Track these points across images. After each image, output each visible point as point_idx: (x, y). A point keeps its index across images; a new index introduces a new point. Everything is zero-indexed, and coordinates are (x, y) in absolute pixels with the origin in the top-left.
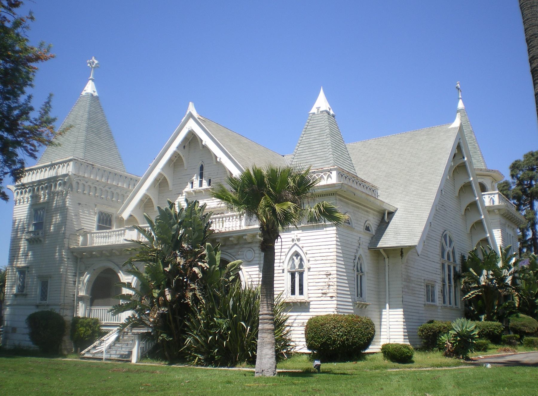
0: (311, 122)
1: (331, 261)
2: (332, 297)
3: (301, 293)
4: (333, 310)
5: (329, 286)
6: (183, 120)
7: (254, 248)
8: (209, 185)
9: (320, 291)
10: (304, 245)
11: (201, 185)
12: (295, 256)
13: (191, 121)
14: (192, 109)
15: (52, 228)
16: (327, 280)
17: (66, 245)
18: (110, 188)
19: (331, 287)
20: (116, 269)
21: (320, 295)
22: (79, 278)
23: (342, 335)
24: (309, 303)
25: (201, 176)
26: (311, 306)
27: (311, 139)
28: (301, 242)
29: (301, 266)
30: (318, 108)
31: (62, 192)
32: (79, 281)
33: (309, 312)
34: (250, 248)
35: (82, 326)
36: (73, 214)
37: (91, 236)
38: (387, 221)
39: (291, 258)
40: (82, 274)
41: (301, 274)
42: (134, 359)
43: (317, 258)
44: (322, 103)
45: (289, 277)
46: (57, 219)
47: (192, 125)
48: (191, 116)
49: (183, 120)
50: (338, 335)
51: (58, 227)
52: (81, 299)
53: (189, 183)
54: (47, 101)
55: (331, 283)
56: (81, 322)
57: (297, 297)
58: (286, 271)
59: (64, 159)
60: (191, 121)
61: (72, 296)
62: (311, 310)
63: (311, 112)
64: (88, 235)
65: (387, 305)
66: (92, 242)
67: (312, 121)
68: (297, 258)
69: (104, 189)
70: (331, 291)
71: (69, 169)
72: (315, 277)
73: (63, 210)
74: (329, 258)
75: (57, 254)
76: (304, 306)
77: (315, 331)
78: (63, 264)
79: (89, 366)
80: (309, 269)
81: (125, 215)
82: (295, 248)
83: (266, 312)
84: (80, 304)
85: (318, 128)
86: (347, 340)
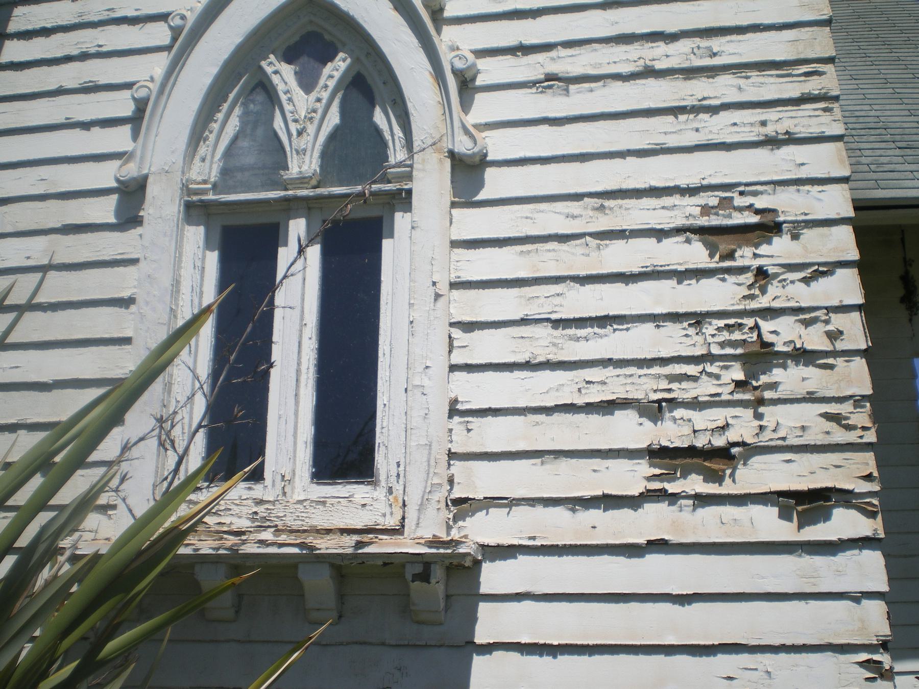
2: (810, 503)
3: (346, 449)
5: (761, 357)
9: (630, 430)
12: (289, 57)
19: (789, 378)
21: (633, 477)
24: (455, 573)
26: (491, 623)
29: (355, 146)
39: (243, 79)
55: (783, 332)
58: (162, 204)
68: (308, 83)
70: (785, 420)
72: (549, 259)
80: (468, 171)
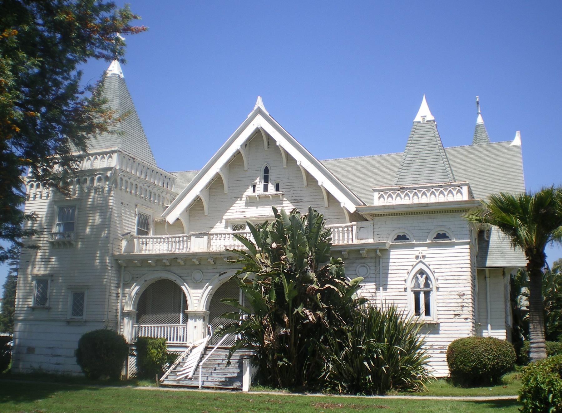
0: (416, 131)
1: (465, 281)
2: (466, 319)
3: (428, 313)
4: (469, 332)
5: (463, 307)
6: (249, 116)
7: (368, 264)
8: (277, 190)
9: (452, 312)
10: (431, 263)
11: (266, 189)
12: (420, 274)
13: (259, 118)
14: (259, 103)
15: (88, 230)
16: (460, 301)
17: (110, 252)
18: (149, 187)
19: (465, 308)
20: (178, 282)
21: (453, 316)
22: (123, 290)
23: (493, 359)
24: (438, 325)
25: (266, 179)
26: (441, 328)
27: (420, 150)
28: (426, 259)
29: (427, 285)
30: (424, 117)
31: (103, 188)
32: (124, 295)
33: (438, 334)
34: (364, 263)
35: (154, 347)
36: (116, 215)
37: (138, 242)
38: (487, 239)
39: (415, 277)
40: (127, 285)
41: (427, 294)
42: (246, 387)
43: (447, 278)
44: (424, 112)
45: (413, 296)
46: (96, 219)
47: (259, 122)
48: (259, 111)
49: (249, 116)
50: (488, 359)
51: (98, 229)
52: (125, 314)
53: (250, 187)
54: (99, 79)
55: (465, 304)
56: (153, 343)
57: (424, 318)
58: (409, 290)
59: (104, 150)
60: (259, 118)
61: (115, 311)
62: (440, 332)
63: (414, 121)
64: (135, 240)
65: (489, 326)
66: (141, 250)
67: (419, 131)
68: (422, 277)
69: (144, 187)
70: (465, 312)
71: (113, 162)
72: (445, 297)
73: (104, 209)
74: (462, 277)
75: (98, 261)
76: (433, 328)
77: (456, 354)
78: (107, 274)
79: (171, 396)
80: (438, 288)
81: (171, 218)
82: (420, 266)
83: (541, 340)
84: (126, 320)
85: (427, 138)
86: (498, 363)
